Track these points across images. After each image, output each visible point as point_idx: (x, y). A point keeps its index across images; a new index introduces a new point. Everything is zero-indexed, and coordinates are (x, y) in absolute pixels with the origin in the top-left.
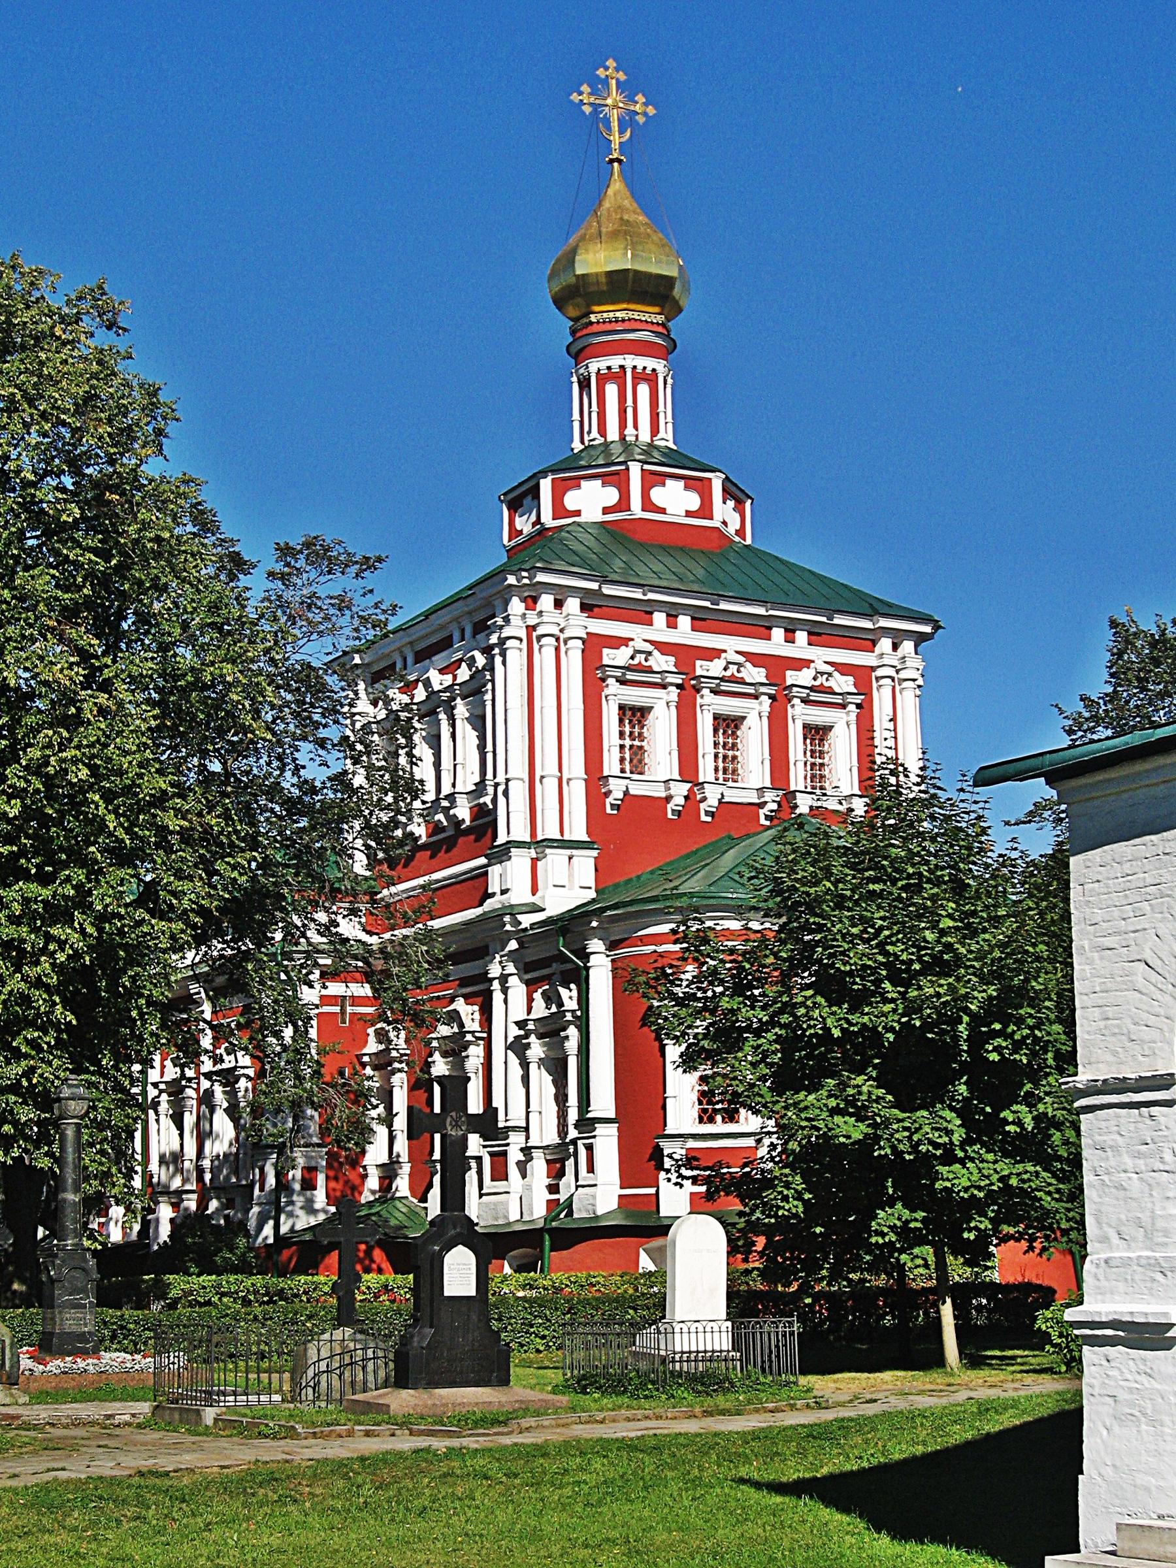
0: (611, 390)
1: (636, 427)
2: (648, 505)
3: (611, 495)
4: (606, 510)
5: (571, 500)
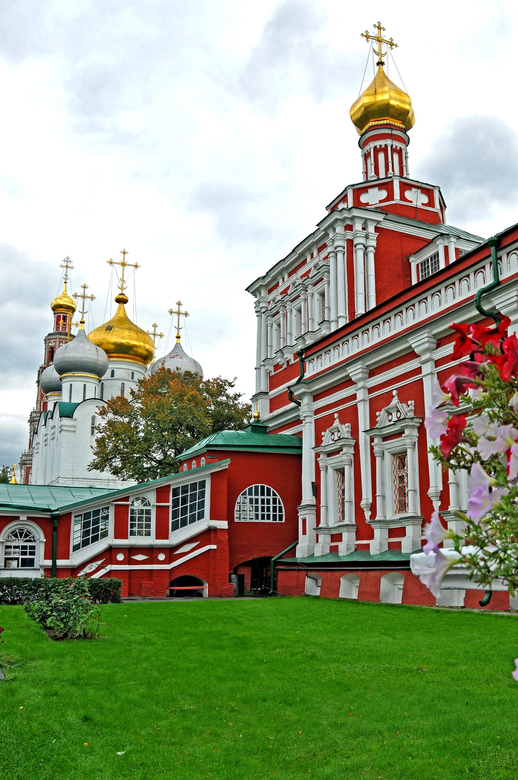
0: (381, 156)
1: (393, 171)
2: (403, 198)
3: (384, 194)
4: (381, 201)
5: (364, 198)
